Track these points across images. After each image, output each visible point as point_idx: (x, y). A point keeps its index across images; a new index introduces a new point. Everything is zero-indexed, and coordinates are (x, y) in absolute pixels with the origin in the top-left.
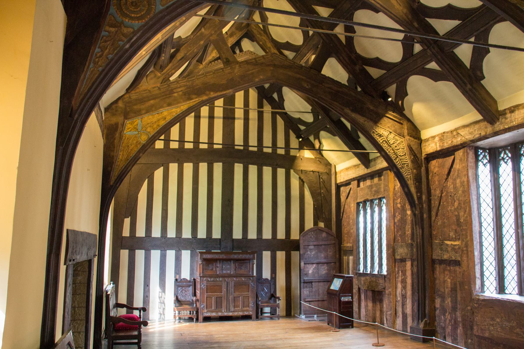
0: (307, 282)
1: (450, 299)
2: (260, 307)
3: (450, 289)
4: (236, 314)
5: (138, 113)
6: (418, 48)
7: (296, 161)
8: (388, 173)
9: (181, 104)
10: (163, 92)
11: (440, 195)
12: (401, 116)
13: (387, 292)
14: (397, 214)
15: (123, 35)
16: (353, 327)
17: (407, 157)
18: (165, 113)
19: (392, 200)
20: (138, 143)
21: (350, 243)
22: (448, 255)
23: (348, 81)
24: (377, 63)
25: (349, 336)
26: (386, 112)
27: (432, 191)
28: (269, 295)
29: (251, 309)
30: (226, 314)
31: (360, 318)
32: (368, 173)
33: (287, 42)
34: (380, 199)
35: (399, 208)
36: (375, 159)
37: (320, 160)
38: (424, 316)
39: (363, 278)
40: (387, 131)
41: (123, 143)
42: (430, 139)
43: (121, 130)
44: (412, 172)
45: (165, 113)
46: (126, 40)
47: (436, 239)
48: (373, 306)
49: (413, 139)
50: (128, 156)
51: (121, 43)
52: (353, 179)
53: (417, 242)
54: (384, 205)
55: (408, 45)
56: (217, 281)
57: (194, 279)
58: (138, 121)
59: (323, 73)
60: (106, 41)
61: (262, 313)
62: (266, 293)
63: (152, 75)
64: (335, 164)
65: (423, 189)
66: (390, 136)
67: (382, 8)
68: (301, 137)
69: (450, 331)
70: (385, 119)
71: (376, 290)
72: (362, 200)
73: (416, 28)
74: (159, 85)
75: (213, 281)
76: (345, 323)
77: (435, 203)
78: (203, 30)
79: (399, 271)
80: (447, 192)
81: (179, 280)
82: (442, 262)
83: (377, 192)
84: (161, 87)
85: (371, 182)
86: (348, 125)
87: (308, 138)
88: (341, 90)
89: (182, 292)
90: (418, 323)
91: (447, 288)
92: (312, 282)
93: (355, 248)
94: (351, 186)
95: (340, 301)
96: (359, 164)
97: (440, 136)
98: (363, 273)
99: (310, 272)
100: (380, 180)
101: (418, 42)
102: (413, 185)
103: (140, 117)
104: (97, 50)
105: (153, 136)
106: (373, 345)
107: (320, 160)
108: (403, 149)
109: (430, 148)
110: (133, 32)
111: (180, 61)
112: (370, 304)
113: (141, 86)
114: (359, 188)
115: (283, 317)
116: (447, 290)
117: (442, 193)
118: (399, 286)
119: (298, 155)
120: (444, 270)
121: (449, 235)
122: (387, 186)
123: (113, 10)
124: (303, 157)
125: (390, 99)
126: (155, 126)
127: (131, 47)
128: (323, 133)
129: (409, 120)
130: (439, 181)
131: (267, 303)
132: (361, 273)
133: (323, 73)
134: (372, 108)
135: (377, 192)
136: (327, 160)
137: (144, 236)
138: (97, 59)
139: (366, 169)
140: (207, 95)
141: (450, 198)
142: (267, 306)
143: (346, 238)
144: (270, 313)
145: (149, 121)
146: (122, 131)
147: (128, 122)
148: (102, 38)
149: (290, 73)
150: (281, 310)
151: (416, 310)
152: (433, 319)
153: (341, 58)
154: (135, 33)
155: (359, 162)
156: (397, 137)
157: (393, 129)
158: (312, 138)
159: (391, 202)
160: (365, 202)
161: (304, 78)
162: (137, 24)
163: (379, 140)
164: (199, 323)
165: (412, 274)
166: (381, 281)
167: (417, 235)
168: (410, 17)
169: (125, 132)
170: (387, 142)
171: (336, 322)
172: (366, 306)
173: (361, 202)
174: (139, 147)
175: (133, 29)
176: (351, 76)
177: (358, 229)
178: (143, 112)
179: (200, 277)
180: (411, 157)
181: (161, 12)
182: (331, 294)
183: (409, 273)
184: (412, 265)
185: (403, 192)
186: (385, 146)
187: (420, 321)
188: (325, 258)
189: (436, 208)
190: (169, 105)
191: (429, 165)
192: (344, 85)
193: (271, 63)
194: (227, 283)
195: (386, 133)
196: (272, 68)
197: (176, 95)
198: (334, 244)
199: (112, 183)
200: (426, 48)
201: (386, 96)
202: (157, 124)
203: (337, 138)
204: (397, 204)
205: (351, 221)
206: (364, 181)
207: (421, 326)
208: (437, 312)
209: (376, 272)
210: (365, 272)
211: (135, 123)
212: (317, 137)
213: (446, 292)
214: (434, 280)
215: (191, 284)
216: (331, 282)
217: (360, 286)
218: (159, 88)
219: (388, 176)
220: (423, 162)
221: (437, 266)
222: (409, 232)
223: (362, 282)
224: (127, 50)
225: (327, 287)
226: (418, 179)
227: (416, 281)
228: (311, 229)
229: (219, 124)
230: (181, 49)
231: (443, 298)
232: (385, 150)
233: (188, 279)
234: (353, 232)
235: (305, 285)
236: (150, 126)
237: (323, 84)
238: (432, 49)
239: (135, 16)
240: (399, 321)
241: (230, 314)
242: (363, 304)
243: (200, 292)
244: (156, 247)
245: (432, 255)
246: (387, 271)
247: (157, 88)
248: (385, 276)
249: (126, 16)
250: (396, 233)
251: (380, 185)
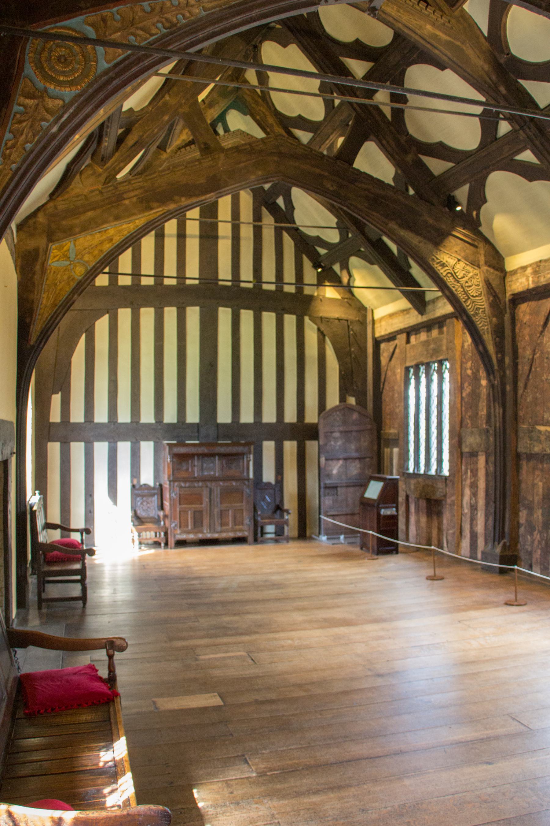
0: (329, 488)
1: (541, 511)
2: (259, 525)
3: (541, 497)
4: (224, 535)
5: (69, 232)
6: (504, 127)
7: (313, 303)
8: (453, 323)
9: (134, 218)
10: (107, 198)
11: (531, 357)
12: (474, 234)
13: (449, 501)
14: (466, 385)
15: (47, 110)
16: (397, 552)
17: (483, 298)
18: (111, 232)
19: (459, 363)
20: (71, 279)
21: (394, 428)
22: (541, 446)
23: (394, 179)
24: (440, 150)
25: (391, 564)
26: (453, 228)
27: (520, 351)
28: (272, 507)
29: (246, 528)
30: (209, 536)
31: (407, 539)
32: (423, 323)
33: (300, 116)
34: (441, 363)
35: (468, 376)
36: (434, 301)
37: (350, 302)
38: (502, 535)
39: (413, 481)
40: (454, 260)
41: (47, 279)
42: (519, 271)
43: (44, 258)
44: (491, 322)
45: (111, 232)
46: (52, 119)
47: (523, 423)
48: (428, 522)
49: (492, 270)
50: (55, 299)
51: (45, 124)
52: (401, 332)
53: (495, 428)
54: (447, 371)
55: (488, 123)
56: (194, 487)
57: (161, 485)
58: (68, 245)
59: (356, 165)
60: (20, 122)
61: (263, 533)
62: (268, 504)
63: (90, 172)
64: (372, 307)
65: (506, 347)
66: (458, 266)
67: (450, 62)
68: (320, 266)
69: (538, 557)
70: (451, 238)
71: (433, 498)
72: (413, 363)
73: (504, 96)
74: (100, 187)
75: (189, 487)
76: (386, 548)
77: (523, 369)
78: (167, 97)
79: (467, 469)
80: (542, 352)
81: (137, 487)
82: (531, 457)
83: (436, 351)
84: (104, 191)
85: (428, 336)
86: (394, 248)
87: (331, 268)
88: (382, 192)
89: (142, 503)
90: (493, 546)
91: (537, 495)
92: (336, 487)
93: (402, 435)
94: (396, 342)
95: (379, 514)
96: (410, 309)
97: (535, 266)
98: (414, 474)
99: (335, 472)
100: (441, 333)
101: (505, 119)
102: (491, 342)
103: (72, 239)
104: (8, 135)
105: (93, 267)
106: (427, 579)
107: (350, 302)
108: (478, 285)
109: (519, 284)
110: (63, 107)
111: (133, 148)
112: (424, 520)
113: (73, 189)
114: (408, 345)
115: (293, 539)
116: (536, 499)
117: (534, 352)
118: (467, 492)
119: (316, 294)
120: (534, 468)
121: (543, 417)
122: (452, 342)
123: (29, 69)
124: (324, 296)
125: (459, 208)
126: (96, 252)
127: (61, 129)
128: (354, 260)
129: (487, 241)
130: (531, 336)
131: (269, 518)
132: (409, 474)
133: (356, 165)
134: (431, 221)
135: (436, 351)
136: (360, 302)
137: (82, 420)
138: (8, 151)
139: (420, 316)
140: (175, 202)
141: (545, 360)
142: (270, 523)
143: (388, 421)
144: (275, 533)
145: (87, 244)
146: (46, 260)
147: (53, 246)
148: (15, 116)
149: (305, 167)
150: (291, 529)
151: (491, 527)
152: (515, 539)
153: (384, 142)
154: (65, 107)
155: (409, 305)
156: (468, 268)
157: (463, 254)
158: (336, 268)
159: (458, 366)
160: (417, 367)
161: (326, 174)
162: (69, 93)
163: (442, 271)
164: (169, 550)
165: (487, 475)
166: (440, 485)
167: (495, 416)
168: (494, 77)
169: (50, 262)
170: (453, 275)
171: (373, 547)
172: (418, 522)
173: (412, 367)
174: (73, 285)
175: (64, 101)
176: (399, 172)
177: (406, 407)
178: (77, 230)
179: (170, 481)
180: (489, 299)
181: (106, 72)
182: (366, 504)
183: (482, 474)
184: (487, 462)
185: (475, 352)
186: (450, 281)
187: (496, 543)
188: (357, 450)
189: (525, 376)
190: (117, 218)
191: (516, 311)
192: (389, 185)
193: (275, 151)
194: (210, 489)
195: (452, 262)
196: (276, 159)
197: (127, 202)
198: (371, 429)
199: (32, 343)
200: (517, 127)
201: (452, 202)
202: (99, 248)
203: (376, 267)
204: (466, 369)
205: (396, 395)
206: (416, 334)
207: (498, 550)
208: (522, 530)
209: (433, 472)
210: (416, 471)
211: (65, 248)
212: (345, 266)
213: (536, 502)
214: (517, 484)
215: (156, 491)
216: (364, 486)
217: (408, 492)
218: (101, 192)
219: (454, 327)
220: (507, 306)
221: (524, 463)
222: (483, 412)
223: (412, 487)
224: (54, 136)
225: (359, 494)
226: (499, 332)
227: (492, 484)
228: (336, 407)
229: (193, 246)
230: (134, 129)
231: (530, 509)
232: (451, 287)
233: (152, 484)
234: (400, 411)
235: (327, 491)
236: (89, 253)
237: (356, 184)
238: (528, 130)
239: (65, 79)
240: (466, 544)
241: (216, 536)
242: (413, 519)
243: (170, 504)
244: (101, 438)
245: (517, 447)
246: (450, 470)
247: (97, 192)
248: (446, 478)
249: (52, 80)
250: (463, 413)
251: (441, 340)
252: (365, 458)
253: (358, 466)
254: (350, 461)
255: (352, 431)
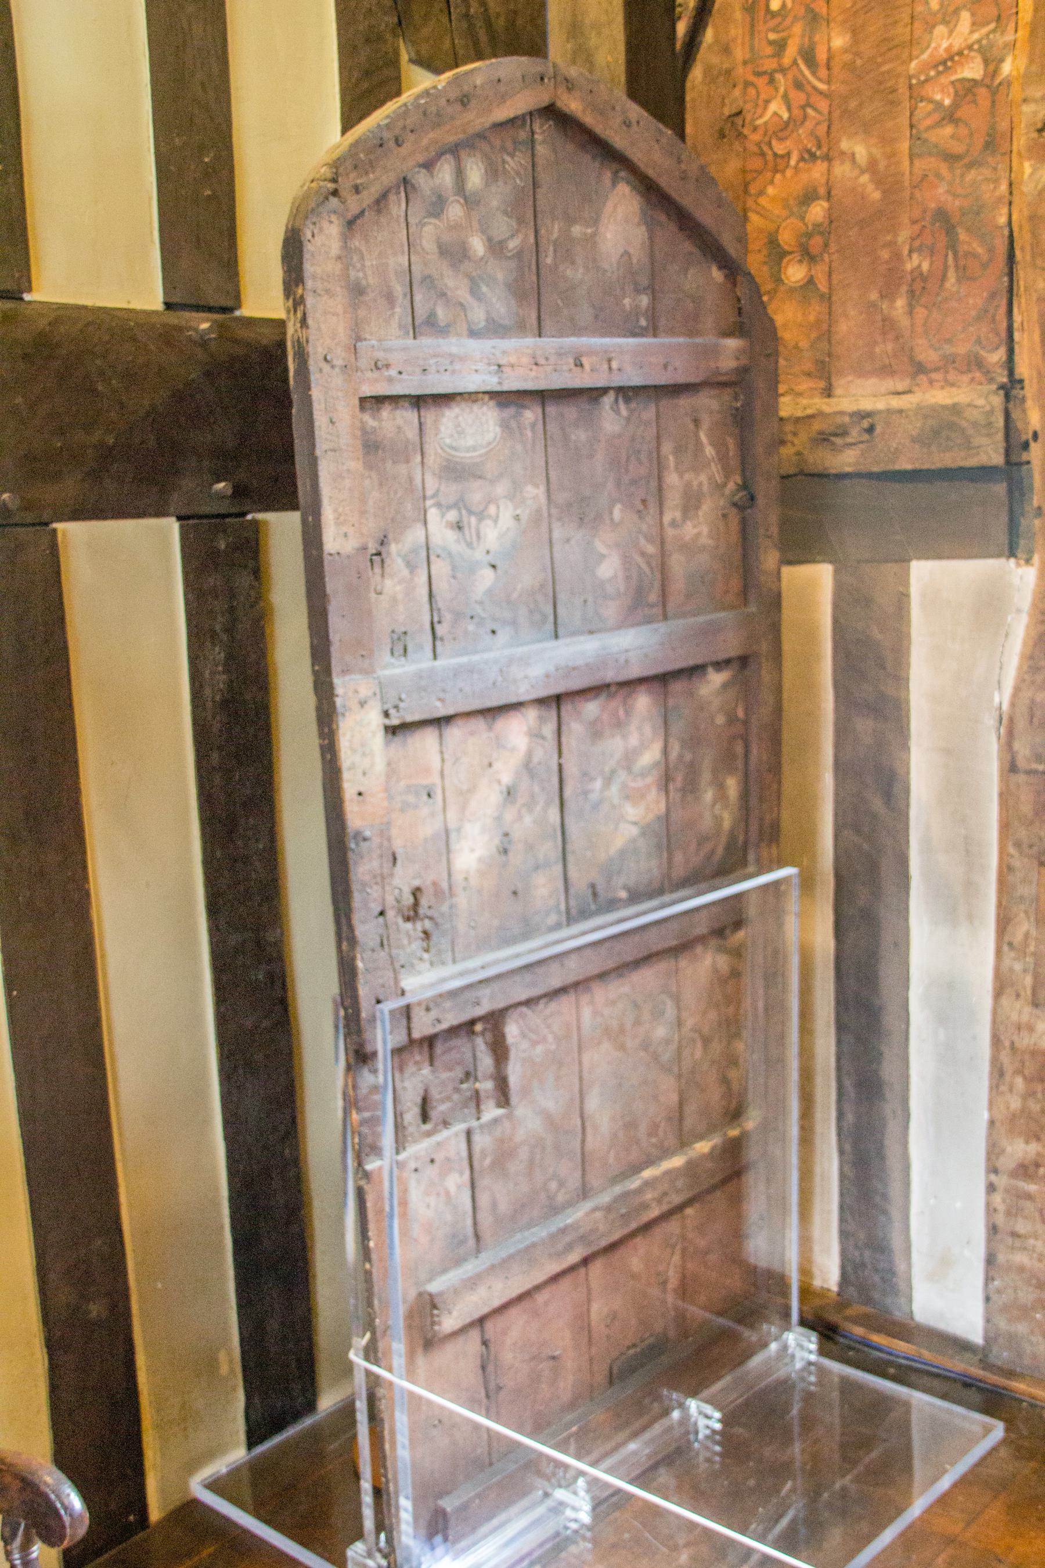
92: (495, 1020)
252: (695, 671)
253: (652, 755)
254: (591, 708)
255: (594, 394)
